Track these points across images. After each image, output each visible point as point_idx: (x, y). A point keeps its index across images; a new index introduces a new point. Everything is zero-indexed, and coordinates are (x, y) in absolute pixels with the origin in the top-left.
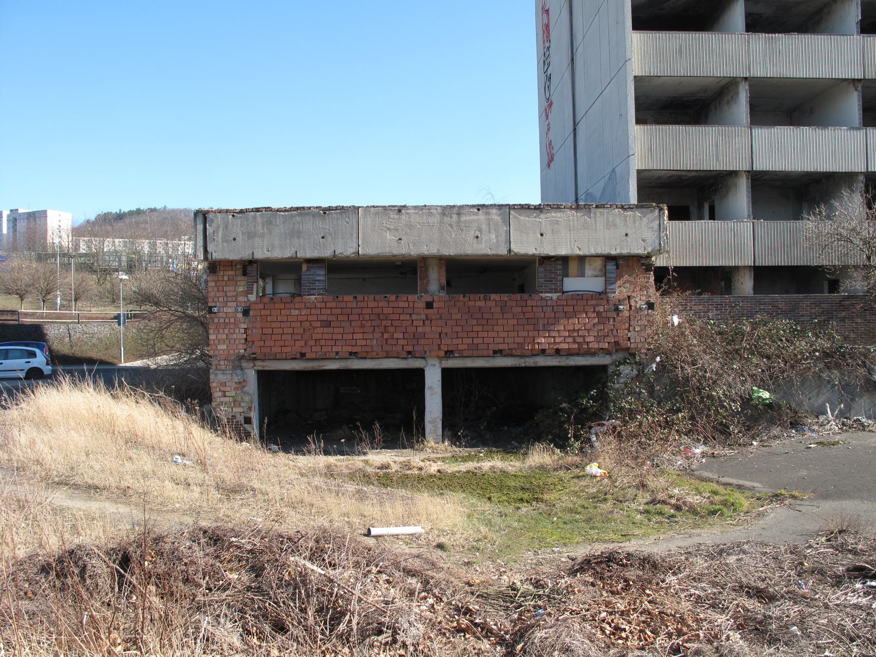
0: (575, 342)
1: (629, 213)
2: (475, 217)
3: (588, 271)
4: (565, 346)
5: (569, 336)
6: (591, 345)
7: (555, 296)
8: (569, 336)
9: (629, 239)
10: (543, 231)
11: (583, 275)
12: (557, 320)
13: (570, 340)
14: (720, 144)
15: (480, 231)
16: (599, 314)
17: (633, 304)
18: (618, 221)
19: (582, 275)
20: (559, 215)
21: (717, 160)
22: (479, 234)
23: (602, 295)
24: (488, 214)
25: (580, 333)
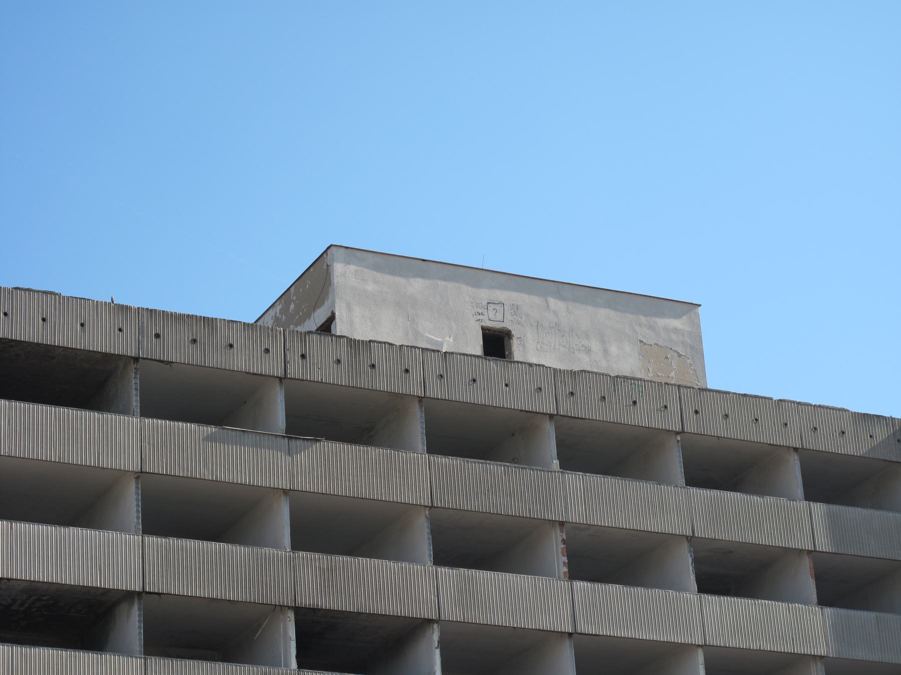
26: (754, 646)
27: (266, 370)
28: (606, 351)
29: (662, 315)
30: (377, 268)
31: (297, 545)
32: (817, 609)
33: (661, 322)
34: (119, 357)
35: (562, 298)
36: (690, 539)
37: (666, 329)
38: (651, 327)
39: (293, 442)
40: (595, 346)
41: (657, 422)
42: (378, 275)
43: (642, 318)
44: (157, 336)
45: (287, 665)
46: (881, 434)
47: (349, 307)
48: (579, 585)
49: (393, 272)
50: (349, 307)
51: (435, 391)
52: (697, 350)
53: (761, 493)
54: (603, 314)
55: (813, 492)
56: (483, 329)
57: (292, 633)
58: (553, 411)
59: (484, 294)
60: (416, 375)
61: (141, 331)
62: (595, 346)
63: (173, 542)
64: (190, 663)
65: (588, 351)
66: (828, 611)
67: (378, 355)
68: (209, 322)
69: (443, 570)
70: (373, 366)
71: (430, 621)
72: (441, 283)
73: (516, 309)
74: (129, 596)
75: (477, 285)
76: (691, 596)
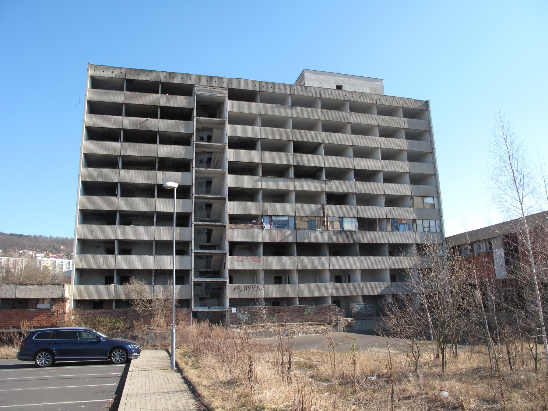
0: (39, 324)
1: (54, 286)
2: (5, 287)
3: (45, 302)
4: (36, 325)
5: (37, 322)
6: (44, 325)
7: (34, 310)
8: (37, 322)
9: (53, 294)
10: (27, 291)
11: (44, 304)
12: (34, 317)
13: (38, 323)
14: (105, 260)
15: (7, 291)
16: (47, 315)
17: (59, 312)
18: (50, 288)
19: (43, 303)
20: (32, 286)
21: (103, 265)
22: (6, 292)
23: (49, 310)
24: (10, 286)
25: (41, 321)
26: (391, 148)
27: (287, 93)
28: (363, 89)
31: (293, 128)
32: (405, 140)
33: (375, 83)
34: (256, 91)
35: (353, 78)
36: (378, 126)
37: (376, 85)
38: (373, 84)
39: (292, 107)
40: (360, 88)
41: (371, 102)
42: (314, 75)
43: (371, 83)
44: (264, 87)
45: (291, 152)
46: (420, 104)
47: (308, 82)
48: (353, 135)
49: (317, 74)
50: (308, 82)
51: (323, 96)
52: (382, 89)
53: (393, 116)
54: (362, 82)
55: (405, 116)
56: (337, 85)
57: (292, 146)
58: (348, 100)
59: (337, 78)
60: (319, 93)
61: (260, 85)
62: (360, 88)
63: (267, 128)
64: (270, 152)
65: (359, 89)
66: (408, 140)
67: (310, 89)
68: (275, 84)
69: (324, 133)
70: (309, 91)
71: (322, 143)
72: (327, 76)
73: (343, 81)
74: (259, 139)
75: (335, 76)
76: (378, 138)
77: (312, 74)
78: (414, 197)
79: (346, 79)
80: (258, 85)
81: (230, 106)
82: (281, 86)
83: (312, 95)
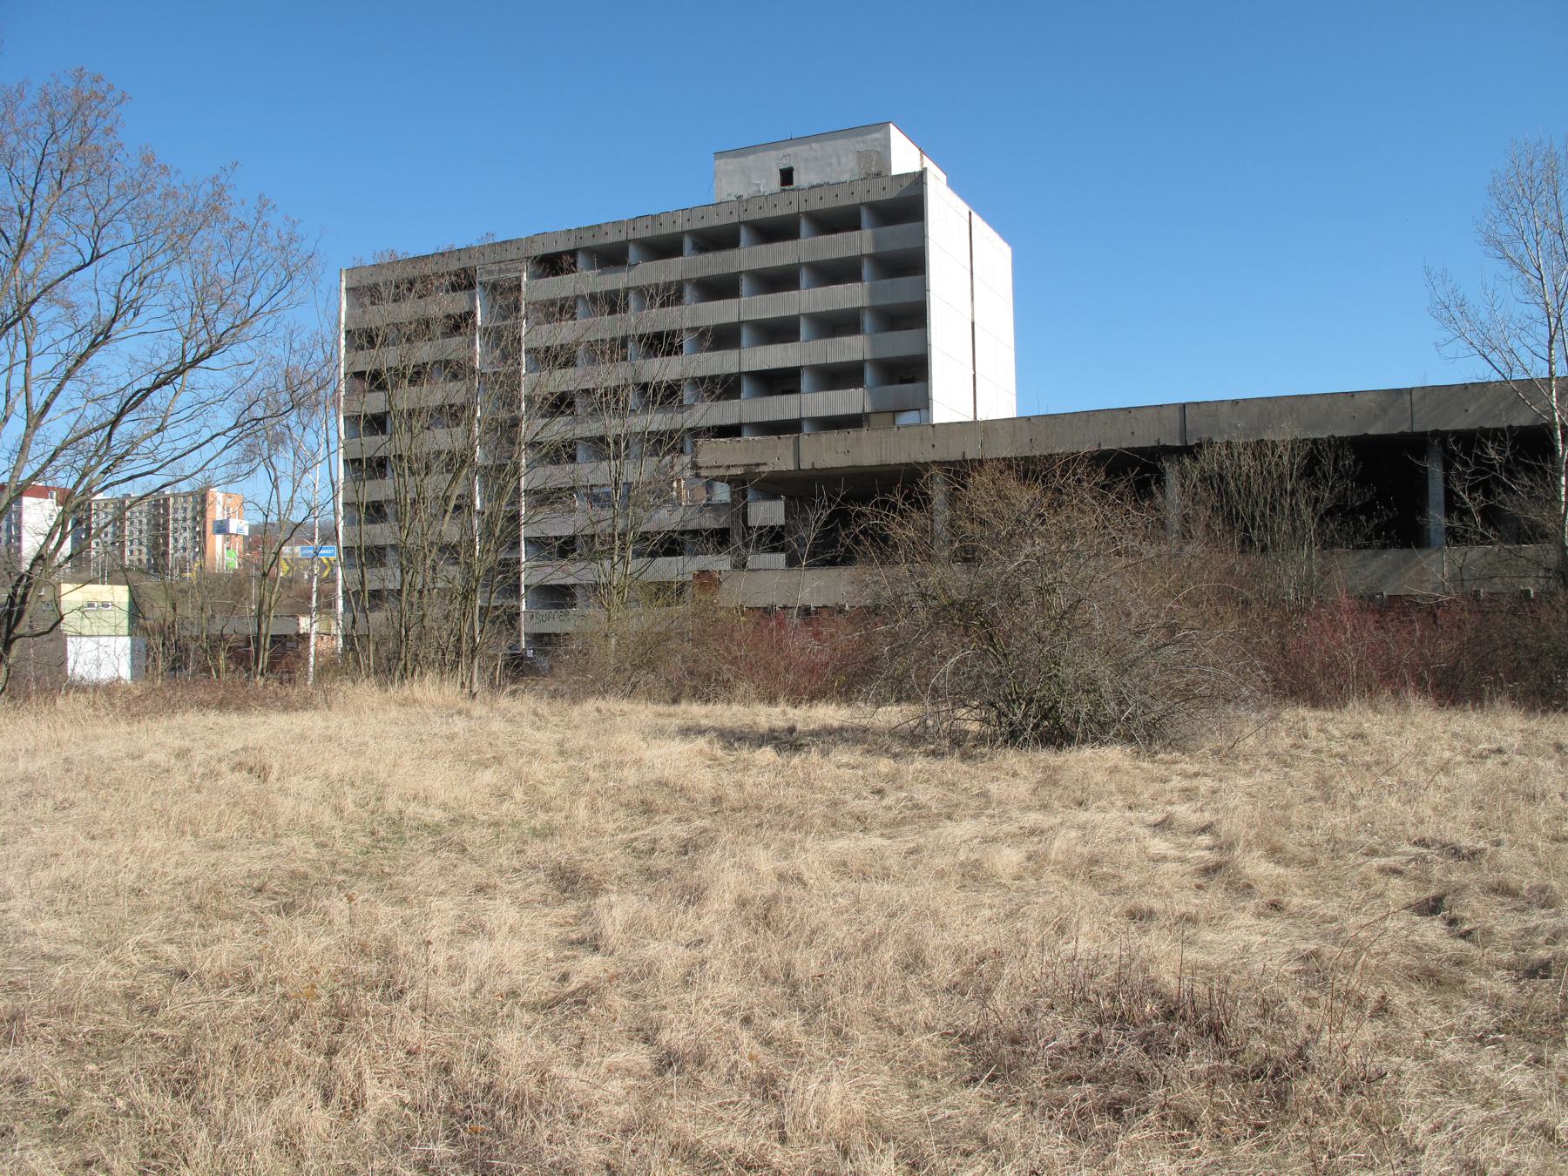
28: (839, 163)
29: (870, 133)
30: (734, 157)
35: (818, 141)
38: (864, 142)
40: (834, 161)
43: (859, 139)
46: (906, 183)
59: (781, 153)
60: (680, 221)
65: (830, 164)
68: (599, 226)
75: (778, 149)
77: (730, 161)
78: (872, 416)
79: (801, 150)
80: (573, 240)
81: (535, 289)
82: (609, 229)
83: (667, 230)
